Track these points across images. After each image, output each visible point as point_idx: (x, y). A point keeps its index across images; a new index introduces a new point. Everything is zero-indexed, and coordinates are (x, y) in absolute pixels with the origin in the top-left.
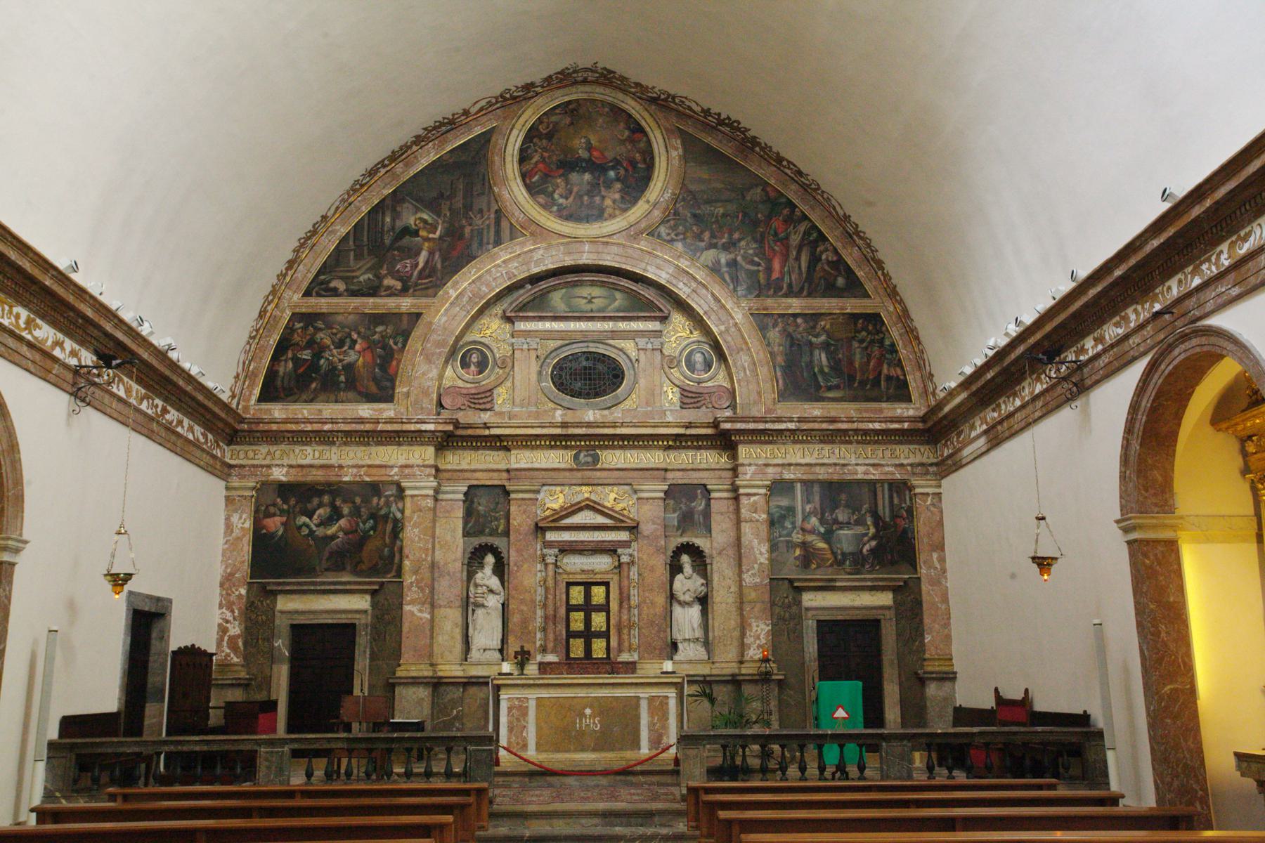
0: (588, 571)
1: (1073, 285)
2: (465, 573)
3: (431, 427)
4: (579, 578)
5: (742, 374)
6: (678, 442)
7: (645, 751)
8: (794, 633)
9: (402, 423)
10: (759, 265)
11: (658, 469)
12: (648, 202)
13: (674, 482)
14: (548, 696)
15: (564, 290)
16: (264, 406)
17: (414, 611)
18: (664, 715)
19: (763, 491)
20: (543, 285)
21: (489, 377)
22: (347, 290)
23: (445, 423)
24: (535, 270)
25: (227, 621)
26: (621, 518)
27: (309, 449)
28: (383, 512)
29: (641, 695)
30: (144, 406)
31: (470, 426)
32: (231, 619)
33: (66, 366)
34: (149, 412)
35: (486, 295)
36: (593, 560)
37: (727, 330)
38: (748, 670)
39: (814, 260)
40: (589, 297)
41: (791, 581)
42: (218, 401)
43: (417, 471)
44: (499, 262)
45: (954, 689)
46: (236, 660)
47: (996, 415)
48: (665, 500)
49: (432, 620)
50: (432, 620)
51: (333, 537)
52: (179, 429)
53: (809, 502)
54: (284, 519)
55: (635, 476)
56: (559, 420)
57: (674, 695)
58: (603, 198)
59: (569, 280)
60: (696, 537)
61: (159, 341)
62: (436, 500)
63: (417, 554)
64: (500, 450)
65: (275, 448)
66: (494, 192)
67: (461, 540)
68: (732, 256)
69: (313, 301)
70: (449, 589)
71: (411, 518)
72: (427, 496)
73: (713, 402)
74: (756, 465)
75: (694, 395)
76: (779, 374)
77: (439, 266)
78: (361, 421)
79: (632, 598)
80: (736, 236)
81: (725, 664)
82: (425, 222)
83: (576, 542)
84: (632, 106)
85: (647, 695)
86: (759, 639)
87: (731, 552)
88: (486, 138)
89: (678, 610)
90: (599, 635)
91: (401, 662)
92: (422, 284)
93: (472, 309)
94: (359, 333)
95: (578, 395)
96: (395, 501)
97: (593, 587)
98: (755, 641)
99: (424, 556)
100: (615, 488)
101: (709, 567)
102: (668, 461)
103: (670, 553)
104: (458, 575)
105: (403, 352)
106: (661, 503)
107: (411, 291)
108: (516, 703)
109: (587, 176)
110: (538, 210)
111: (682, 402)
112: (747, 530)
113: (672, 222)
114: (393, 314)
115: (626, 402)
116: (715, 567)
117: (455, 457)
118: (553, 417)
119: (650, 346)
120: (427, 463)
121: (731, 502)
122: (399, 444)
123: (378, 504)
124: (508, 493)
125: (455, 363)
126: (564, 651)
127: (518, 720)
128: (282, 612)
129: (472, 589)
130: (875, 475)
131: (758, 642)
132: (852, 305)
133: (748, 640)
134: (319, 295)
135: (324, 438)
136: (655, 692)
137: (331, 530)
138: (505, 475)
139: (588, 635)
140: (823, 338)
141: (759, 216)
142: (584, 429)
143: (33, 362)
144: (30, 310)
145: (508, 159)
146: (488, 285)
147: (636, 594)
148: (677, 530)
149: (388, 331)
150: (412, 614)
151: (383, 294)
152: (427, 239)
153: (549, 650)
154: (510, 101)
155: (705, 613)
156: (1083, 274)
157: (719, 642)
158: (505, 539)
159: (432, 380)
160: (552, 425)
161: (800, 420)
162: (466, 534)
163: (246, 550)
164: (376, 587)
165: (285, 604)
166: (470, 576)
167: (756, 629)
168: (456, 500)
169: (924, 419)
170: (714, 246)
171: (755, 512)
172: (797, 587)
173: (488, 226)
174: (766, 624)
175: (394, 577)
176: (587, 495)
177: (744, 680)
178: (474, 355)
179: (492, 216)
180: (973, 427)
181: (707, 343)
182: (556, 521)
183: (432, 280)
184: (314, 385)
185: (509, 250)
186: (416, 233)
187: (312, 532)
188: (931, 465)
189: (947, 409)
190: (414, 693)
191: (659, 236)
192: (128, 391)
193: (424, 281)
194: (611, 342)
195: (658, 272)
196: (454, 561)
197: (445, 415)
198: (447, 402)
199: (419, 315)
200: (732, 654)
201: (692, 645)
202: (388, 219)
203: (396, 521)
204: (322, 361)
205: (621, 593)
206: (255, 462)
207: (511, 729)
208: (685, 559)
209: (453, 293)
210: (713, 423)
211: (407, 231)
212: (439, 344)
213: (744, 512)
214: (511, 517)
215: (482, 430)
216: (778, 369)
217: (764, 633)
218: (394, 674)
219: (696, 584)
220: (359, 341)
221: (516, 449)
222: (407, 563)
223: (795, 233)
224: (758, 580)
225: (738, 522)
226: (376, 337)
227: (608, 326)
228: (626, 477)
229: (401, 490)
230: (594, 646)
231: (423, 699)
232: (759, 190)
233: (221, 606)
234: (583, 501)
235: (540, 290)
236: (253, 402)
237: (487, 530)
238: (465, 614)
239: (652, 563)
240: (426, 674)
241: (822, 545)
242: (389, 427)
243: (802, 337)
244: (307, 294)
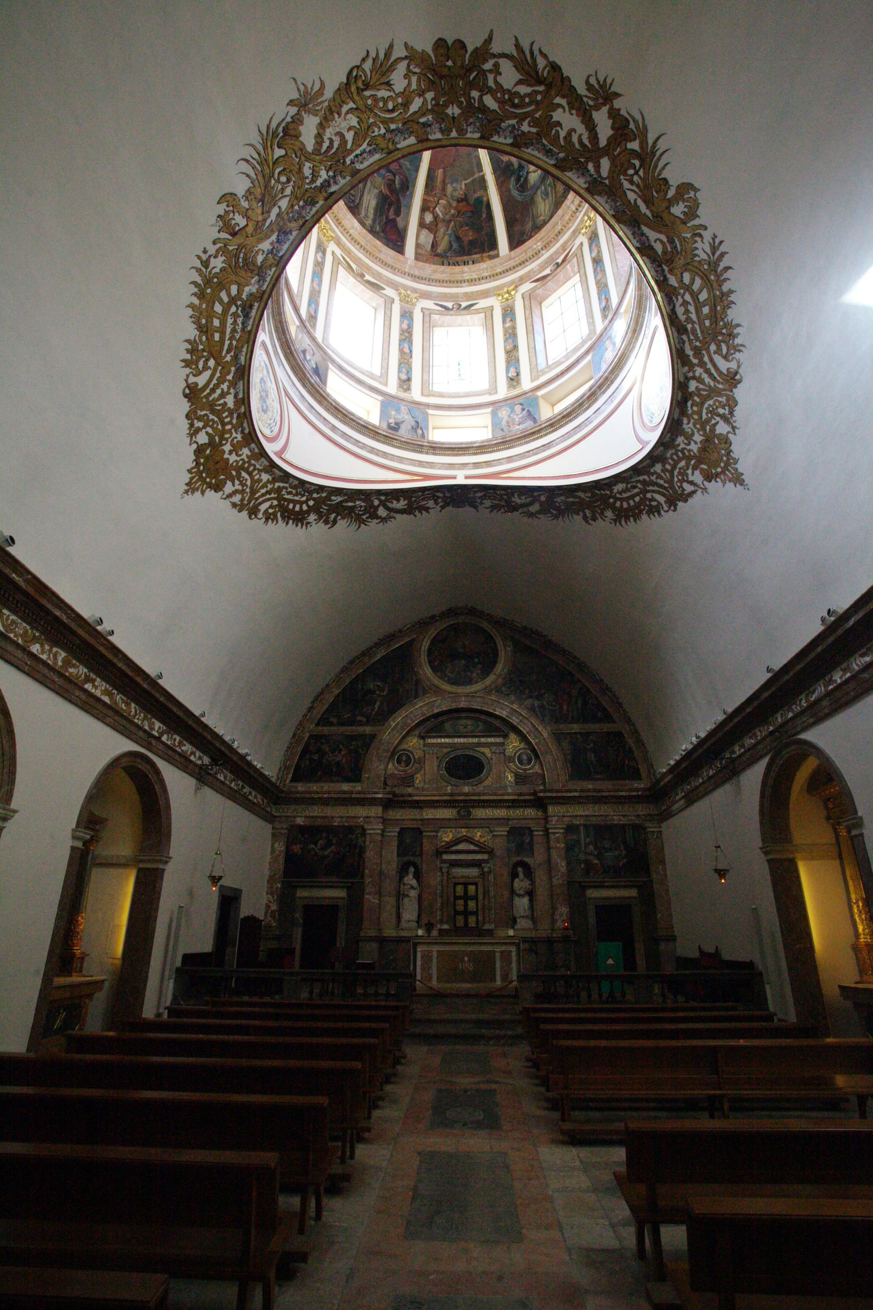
1: (725, 716)
3: (380, 796)
4: (462, 880)
5: (548, 767)
6: (514, 804)
7: (499, 983)
10: (555, 706)
16: (294, 784)
17: (370, 899)
19: (562, 831)
20: (440, 719)
21: (412, 768)
22: (338, 723)
24: (436, 711)
25: (270, 902)
27: (316, 808)
30: (233, 785)
31: (402, 796)
32: (272, 901)
33: (195, 765)
34: (235, 788)
37: (540, 741)
41: (580, 883)
42: (270, 781)
45: (675, 945)
46: (274, 924)
47: (689, 787)
48: (507, 836)
49: (380, 904)
50: (380, 904)
51: (327, 857)
52: (250, 797)
53: (588, 836)
54: (302, 846)
56: (449, 791)
58: (472, 672)
61: (242, 751)
62: (382, 835)
65: (298, 807)
67: (396, 859)
69: (320, 728)
70: (389, 886)
72: (378, 834)
78: (344, 792)
80: (543, 692)
81: (544, 931)
82: (379, 686)
84: (485, 625)
85: (499, 950)
88: (411, 642)
89: (516, 899)
90: (472, 913)
93: (403, 732)
94: (343, 745)
95: (459, 778)
101: (533, 874)
103: (511, 866)
106: (505, 838)
109: (463, 662)
113: (508, 685)
117: (394, 812)
118: (446, 790)
119: (498, 751)
120: (379, 815)
122: (364, 805)
124: (421, 833)
128: (300, 898)
129: (402, 886)
130: (624, 821)
132: (606, 727)
134: (323, 725)
135: (325, 802)
136: (504, 948)
137: (327, 852)
138: (420, 822)
139: (466, 913)
140: (592, 745)
143: (181, 763)
144: (181, 737)
145: (422, 653)
146: (411, 720)
152: (379, 696)
154: (423, 624)
155: (531, 901)
156: (730, 710)
160: (445, 795)
161: (582, 791)
162: (398, 855)
163: (281, 861)
164: (349, 885)
165: (302, 893)
166: (401, 879)
169: (649, 789)
170: (531, 697)
171: (558, 843)
176: (464, 834)
179: (414, 683)
180: (677, 794)
182: (448, 848)
183: (383, 717)
184: (319, 773)
186: (374, 692)
187: (316, 854)
188: (655, 815)
189: (662, 784)
191: (502, 692)
192: (225, 777)
194: (477, 749)
195: (501, 711)
197: (388, 789)
198: (389, 782)
202: (360, 686)
203: (361, 847)
204: (324, 760)
205: (484, 889)
206: (288, 814)
207: (423, 969)
208: (520, 869)
209: (393, 724)
211: (370, 692)
219: (527, 884)
222: (367, 871)
225: (549, 849)
226: (352, 747)
227: (476, 740)
228: (484, 824)
229: (364, 830)
230: (470, 920)
233: (267, 894)
236: (288, 782)
241: (596, 861)
242: (358, 796)
244: (318, 725)
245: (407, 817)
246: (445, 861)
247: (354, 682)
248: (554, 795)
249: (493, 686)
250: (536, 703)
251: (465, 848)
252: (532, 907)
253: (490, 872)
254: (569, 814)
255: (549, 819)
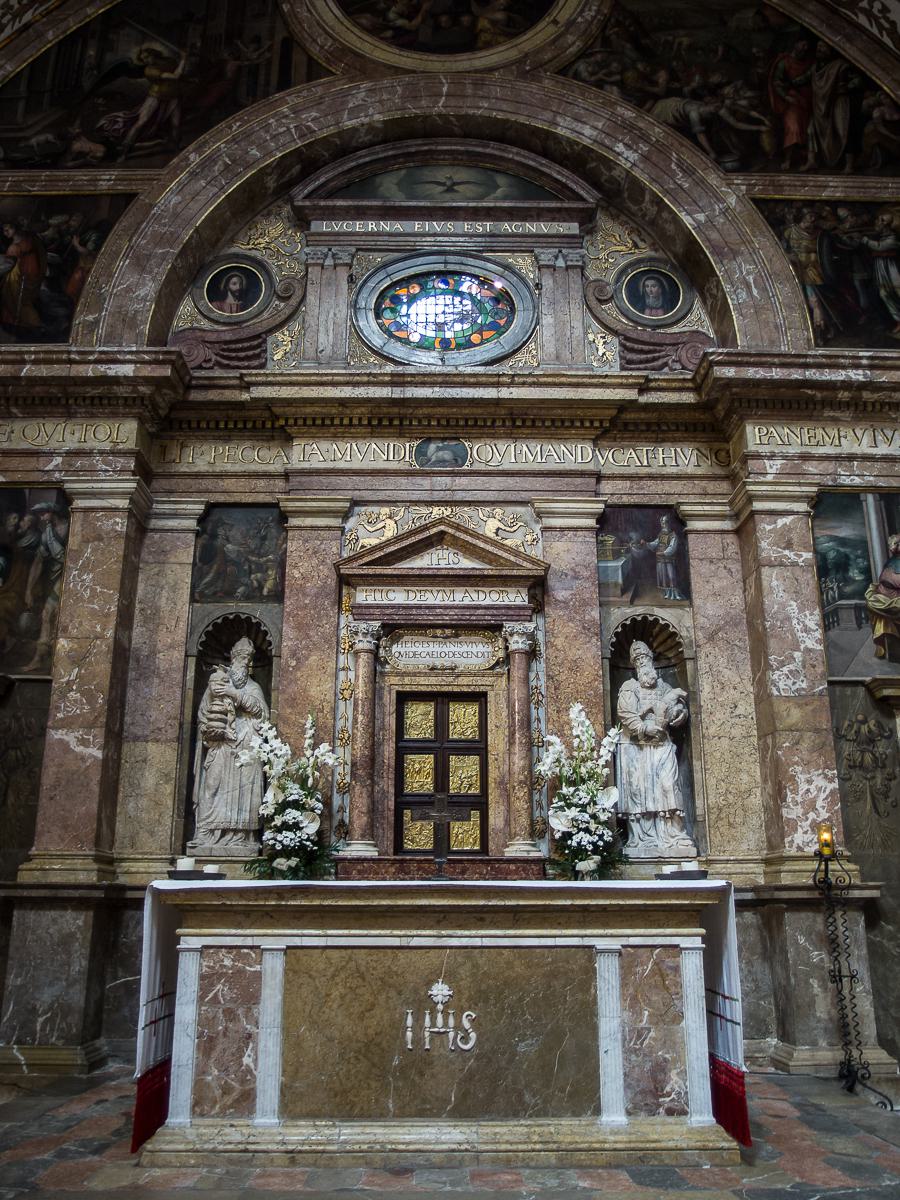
0: (444, 669)
2: (191, 674)
3: (128, 370)
5: (744, 295)
7: (614, 1116)
8: (887, 797)
9: (71, 362)
10: (759, 122)
11: (582, 474)
12: (555, 22)
13: (614, 500)
14: (321, 942)
15: (403, 172)
18: (668, 1006)
23: (157, 362)
26: (512, 558)
28: (25, 542)
29: (600, 943)
35: (257, 161)
36: (453, 649)
37: (710, 220)
38: (797, 876)
39: (858, 119)
40: (448, 183)
41: (870, 688)
43: (98, 462)
44: (285, 109)
48: (598, 532)
55: (538, 487)
57: (698, 942)
59: (413, 150)
60: (662, 606)
63: (86, 626)
64: (272, 438)
66: (282, 14)
68: (711, 108)
71: (79, 553)
72: (116, 509)
73: (684, 359)
74: (785, 457)
75: (646, 348)
76: (813, 299)
77: (176, 121)
79: (534, 725)
80: (715, 79)
82: (157, 55)
83: (419, 607)
85: (616, 944)
86: (814, 809)
87: (741, 637)
91: (34, 851)
92: (140, 148)
94: (18, 228)
96: (51, 521)
97: (452, 706)
98: (805, 814)
99: (98, 629)
100: (498, 510)
101: (689, 665)
102: (602, 462)
104: (178, 676)
105: (95, 258)
107: (120, 160)
108: (228, 962)
110: (360, 34)
111: (621, 358)
112: (774, 583)
114: (83, 196)
115: (519, 356)
116: (702, 664)
120: (121, 446)
121: (731, 539)
123: (17, 526)
125: (196, 291)
126: (390, 835)
127: (230, 1015)
129: (204, 705)
131: (812, 815)
133: (791, 812)
136: (638, 936)
138: (280, 484)
140: (889, 241)
141: (754, 50)
142: (437, 389)
146: (259, 147)
147: (542, 716)
148: (624, 591)
149: (72, 223)
150: (65, 746)
151: (70, 164)
152: (159, 81)
153: (357, 832)
155: (683, 756)
157: (719, 818)
158: (274, 607)
159: (144, 299)
160: (374, 381)
167: (806, 787)
168: (184, 531)
170: (678, 93)
171: (789, 546)
172: (886, 698)
173: (269, 62)
174: (826, 777)
175: (36, 671)
177: (788, 901)
178: (235, 279)
181: (666, 262)
185: (305, 93)
190: (54, 921)
191: (576, 76)
193: (146, 144)
195: (578, 126)
196: (171, 647)
199: (130, 197)
200: (749, 840)
201: (661, 825)
207: (206, 1045)
208: (639, 648)
209: (194, 158)
210: (693, 380)
211: (125, 69)
212: (160, 240)
213: (767, 548)
214: (289, 561)
215: (237, 392)
216: (809, 290)
217: (823, 796)
218: (14, 874)
219: (667, 700)
220: (17, 240)
221: (302, 436)
222: (63, 644)
223: (821, 77)
224: (804, 685)
226: (48, 233)
229: (65, 498)
231: (72, 935)
232: (750, 13)
234: (434, 524)
235: (358, 167)
237: (241, 590)
238: (186, 756)
239: (573, 654)
240: (82, 878)
243: (851, 238)
245: (238, 468)
246: (361, 612)
247: (69, 44)
248: (776, 374)
249: (547, 56)
250: (694, 112)
251: (443, 563)
252: (687, 784)
253: (532, 654)
254: (821, 451)
255: (752, 464)
